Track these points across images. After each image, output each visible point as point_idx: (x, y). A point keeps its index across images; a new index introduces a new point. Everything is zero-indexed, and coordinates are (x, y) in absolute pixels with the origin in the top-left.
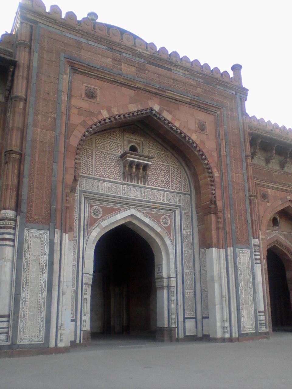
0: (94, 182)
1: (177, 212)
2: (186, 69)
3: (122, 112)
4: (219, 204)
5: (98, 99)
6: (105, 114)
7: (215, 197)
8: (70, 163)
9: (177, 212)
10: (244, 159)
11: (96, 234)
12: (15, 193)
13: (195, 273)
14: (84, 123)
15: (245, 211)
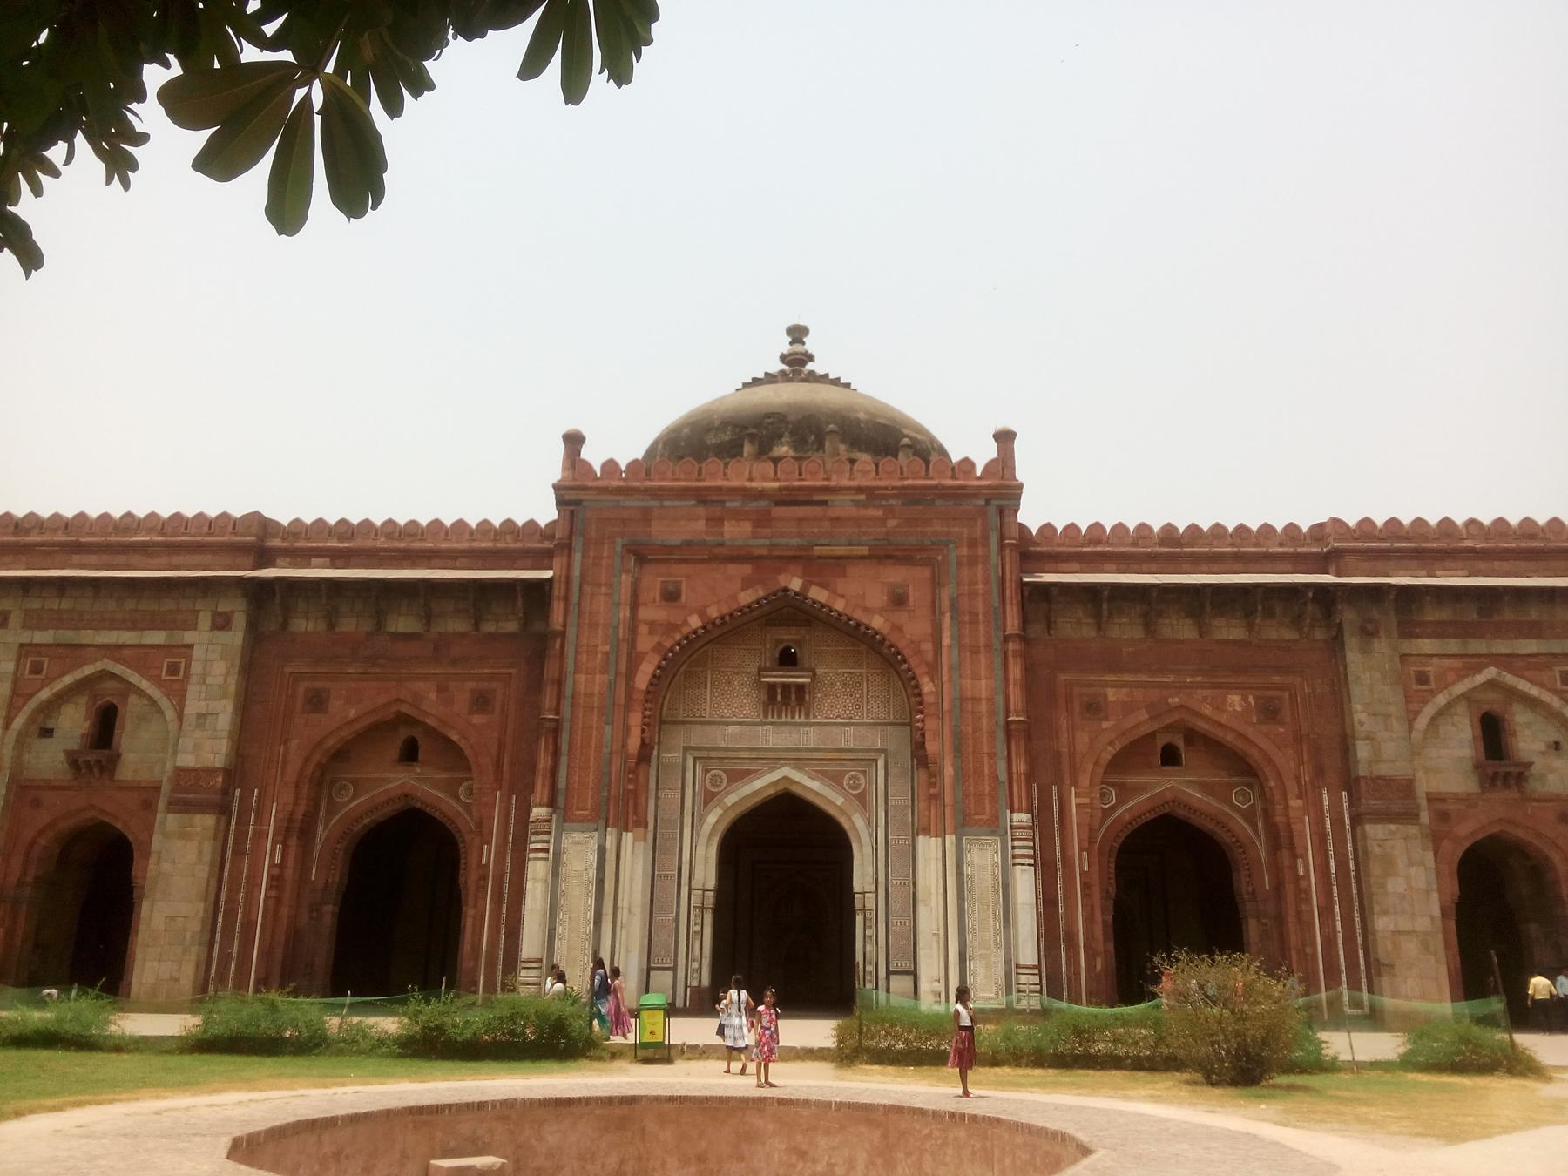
0: (709, 729)
1: (881, 763)
2: (859, 490)
3: (725, 610)
4: (931, 747)
5: (683, 598)
6: (695, 622)
7: (923, 735)
8: (636, 719)
9: (881, 763)
10: (997, 645)
11: (715, 820)
12: (547, 782)
13: (914, 884)
14: (658, 648)
15: (992, 755)
